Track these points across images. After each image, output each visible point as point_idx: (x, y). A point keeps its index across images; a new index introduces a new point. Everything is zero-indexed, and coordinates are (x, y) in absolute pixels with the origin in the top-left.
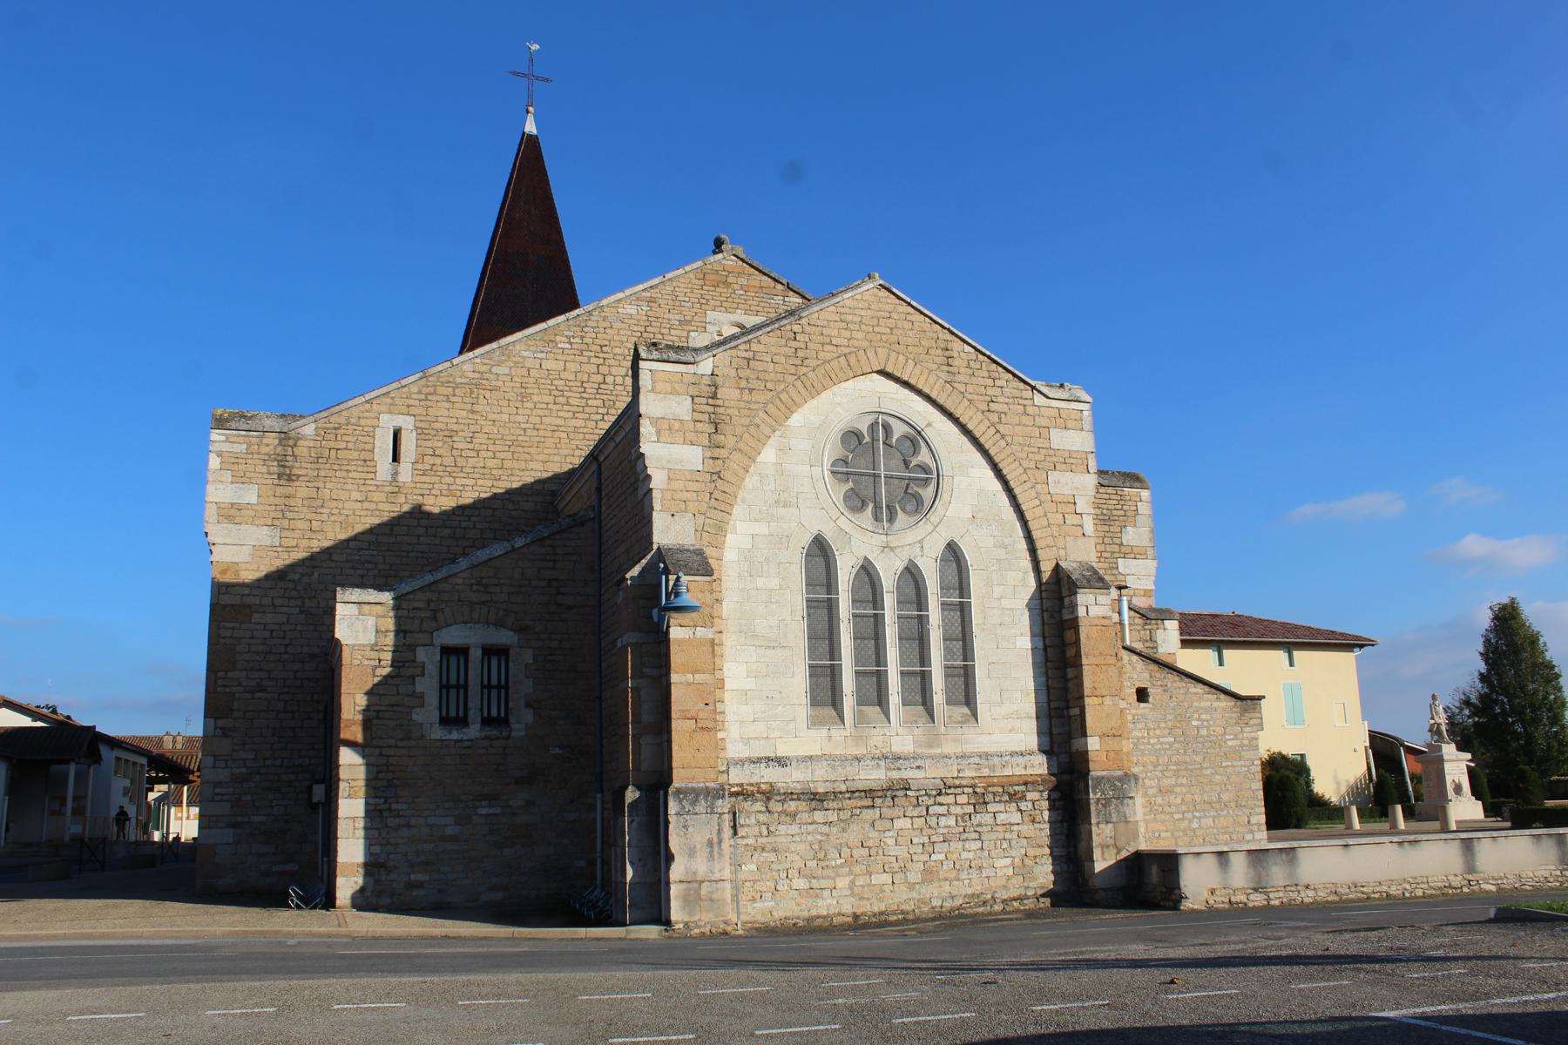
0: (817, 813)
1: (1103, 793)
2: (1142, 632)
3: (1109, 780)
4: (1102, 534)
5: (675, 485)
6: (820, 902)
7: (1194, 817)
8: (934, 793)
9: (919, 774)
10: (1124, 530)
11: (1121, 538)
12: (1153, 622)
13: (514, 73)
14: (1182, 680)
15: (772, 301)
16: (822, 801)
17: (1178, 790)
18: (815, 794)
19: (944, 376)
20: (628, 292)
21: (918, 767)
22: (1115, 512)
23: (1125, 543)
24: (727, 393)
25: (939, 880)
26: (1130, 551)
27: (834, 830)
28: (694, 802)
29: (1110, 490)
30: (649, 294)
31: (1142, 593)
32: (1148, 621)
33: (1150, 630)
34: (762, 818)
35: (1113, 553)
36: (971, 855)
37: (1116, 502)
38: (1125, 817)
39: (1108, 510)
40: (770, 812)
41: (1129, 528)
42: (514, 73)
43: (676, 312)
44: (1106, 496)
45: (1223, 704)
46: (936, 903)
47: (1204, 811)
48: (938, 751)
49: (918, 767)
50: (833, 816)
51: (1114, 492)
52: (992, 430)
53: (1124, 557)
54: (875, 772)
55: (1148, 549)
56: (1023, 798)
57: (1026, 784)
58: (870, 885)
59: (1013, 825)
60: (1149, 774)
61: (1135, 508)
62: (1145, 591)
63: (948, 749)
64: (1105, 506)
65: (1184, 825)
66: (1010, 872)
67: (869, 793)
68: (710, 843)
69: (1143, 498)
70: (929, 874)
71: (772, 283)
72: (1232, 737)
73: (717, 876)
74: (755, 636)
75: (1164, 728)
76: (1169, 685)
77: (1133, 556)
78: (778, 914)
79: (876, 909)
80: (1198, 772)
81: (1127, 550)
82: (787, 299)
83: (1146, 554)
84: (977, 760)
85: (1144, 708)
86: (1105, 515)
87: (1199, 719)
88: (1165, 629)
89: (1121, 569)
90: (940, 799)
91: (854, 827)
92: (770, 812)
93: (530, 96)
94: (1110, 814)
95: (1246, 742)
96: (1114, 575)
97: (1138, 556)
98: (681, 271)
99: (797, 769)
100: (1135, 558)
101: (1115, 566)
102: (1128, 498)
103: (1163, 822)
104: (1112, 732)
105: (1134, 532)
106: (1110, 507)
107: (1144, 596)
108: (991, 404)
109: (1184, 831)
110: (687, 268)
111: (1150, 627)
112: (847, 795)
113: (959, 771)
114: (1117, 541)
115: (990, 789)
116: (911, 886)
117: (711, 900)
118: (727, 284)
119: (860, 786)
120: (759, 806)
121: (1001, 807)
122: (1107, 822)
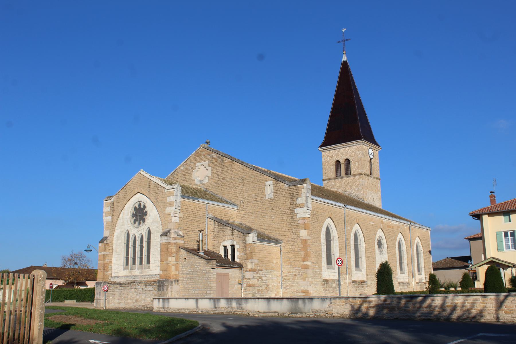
0: (121, 287)
2: (243, 238)
3: (161, 281)
4: (290, 202)
6: (120, 305)
7: (193, 291)
10: (297, 199)
11: (296, 202)
12: (246, 234)
13: (339, 42)
14: (194, 256)
16: (121, 285)
17: (190, 283)
18: (120, 283)
19: (148, 190)
21: (138, 278)
22: (295, 194)
23: (297, 203)
24: (115, 204)
26: (299, 206)
27: (123, 291)
28: (98, 285)
29: (294, 187)
30: (186, 163)
31: (302, 219)
33: (245, 237)
34: (113, 288)
36: (143, 297)
37: (295, 190)
40: (114, 287)
41: (299, 198)
42: (339, 42)
44: (292, 189)
45: (203, 261)
46: (137, 307)
47: (196, 289)
48: (142, 274)
49: (138, 278)
50: (123, 288)
51: (295, 187)
52: (156, 200)
56: (153, 285)
57: (154, 282)
63: (144, 274)
64: (292, 193)
65: (190, 293)
66: (150, 301)
67: (129, 283)
68: (100, 293)
70: (137, 301)
72: (204, 270)
75: (189, 268)
76: (191, 257)
77: (300, 207)
78: (114, 307)
79: (128, 307)
80: (195, 279)
82: (212, 155)
83: (304, 206)
84: (147, 276)
86: (292, 195)
87: (197, 265)
88: (249, 236)
89: (295, 212)
90: (139, 285)
91: (125, 290)
92: (114, 287)
93: (344, 48)
95: (208, 271)
98: (191, 155)
102: (299, 188)
104: (164, 270)
109: (191, 294)
113: (144, 279)
114: (295, 203)
115: (148, 283)
117: (99, 303)
118: (200, 155)
119: (127, 282)
120: (113, 286)
121: (149, 287)
122: (160, 291)
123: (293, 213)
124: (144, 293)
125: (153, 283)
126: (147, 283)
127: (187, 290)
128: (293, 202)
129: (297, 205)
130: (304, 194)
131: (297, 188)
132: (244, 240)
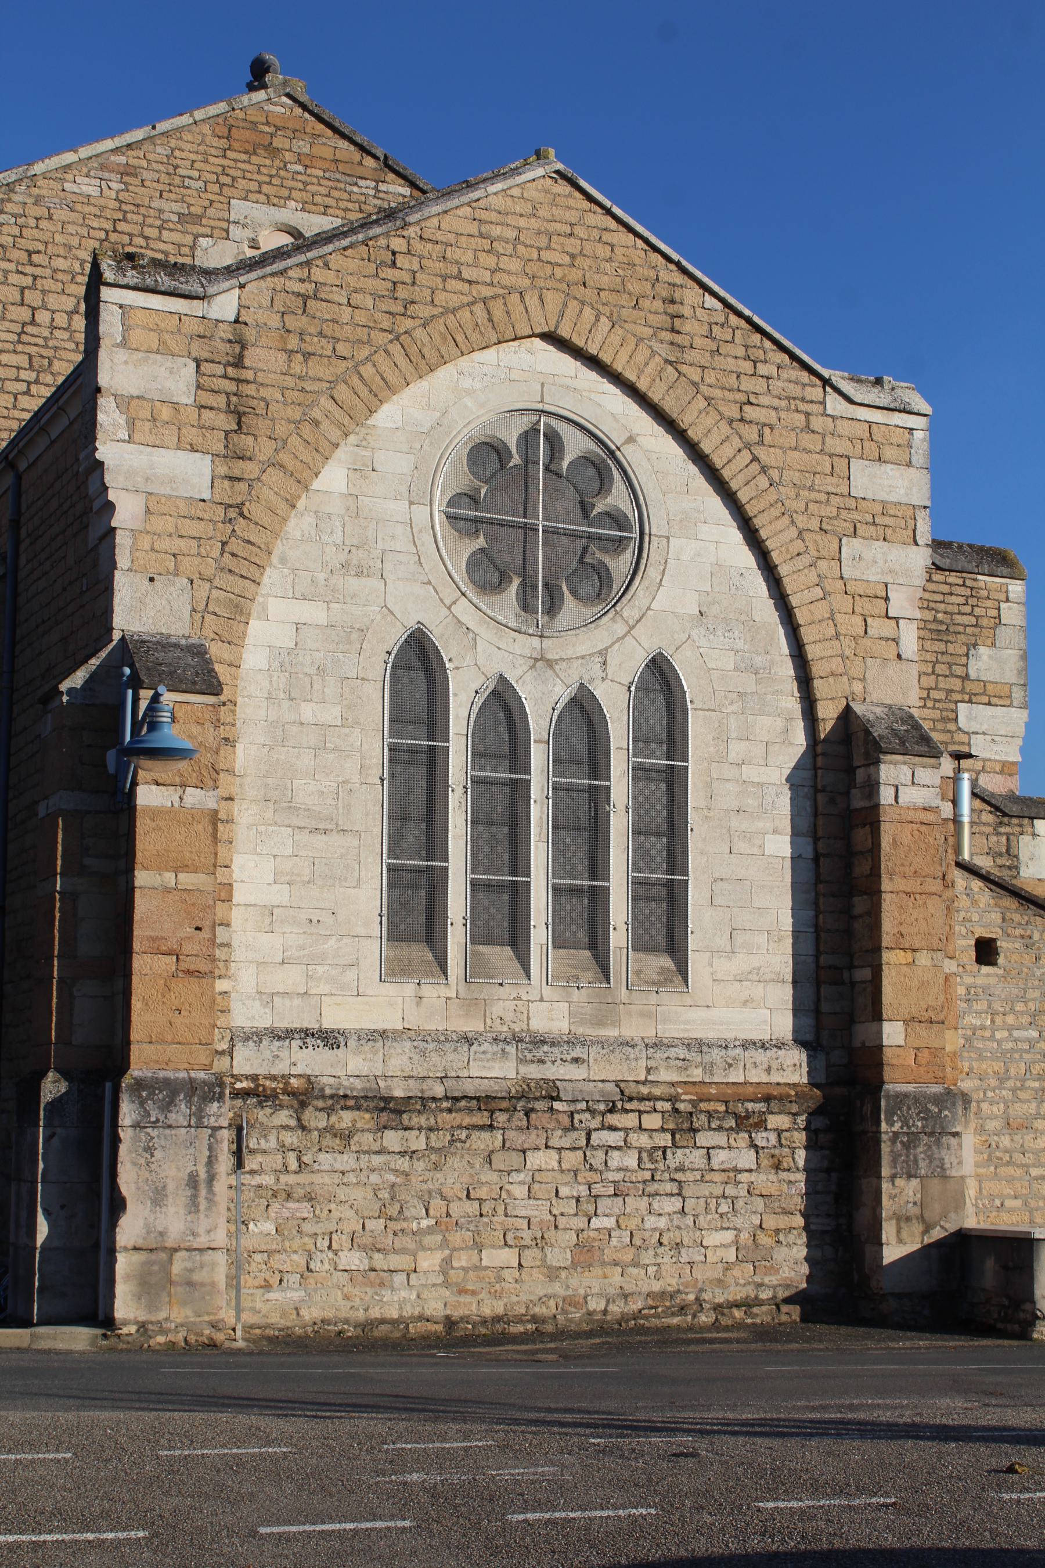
0: (389, 1134)
1: (905, 1123)
2: (993, 839)
3: (916, 1100)
4: (930, 657)
5: (159, 524)
6: (387, 1295)
8: (602, 1107)
9: (577, 1073)
10: (972, 652)
11: (966, 665)
12: (1015, 821)
15: (355, 189)
16: (400, 1112)
19: (664, 350)
20: (84, 152)
21: (576, 1060)
22: (959, 619)
23: (973, 675)
25: (604, 1264)
27: (420, 1165)
28: (167, 1106)
29: (953, 578)
30: (122, 159)
31: (998, 769)
32: (1006, 820)
33: (1008, 835)
34: (291, 1139)
35: (950, 691)
36: (662, 1223)
37: (961, 600)
38: (942, 1167)
39: (945, 613)
40: (303, 1128)
41: (982, 649)
43: (173, 196)
44: (945, 588)
46: (596, 1304)
48: (612, 1033)
49: (576, 1060)
50: (417, 1141)
51: (960, 582)
52: (746, 456)
53: (970, 701)
54: (497, 1065)
55: (1015, 689)
57: (767, 1099)
58: (478, 1268)
59: (740, 1171)
60: (990, 1094)
61: (995, 613)
62: (1004, 764)
63: (632, 1029)
64: (942, 607)
67: (485, 1102)
68: (193, 1181)
69: (1011, 596)
71: (357, 155)
73: (202, 1241)
74: (292, 809)
75: (1022, 1013)
77: (985, 700)
78: (311, 1313)
79: (487, 1312)
81: (976, 688)
82: (382, 187)
83: (1010, 697)
84: (682, 1053)
85: (988, 975)
86: (941, 622)
88: (1034, 835)
89: (962, 722)
90: (613, 1119)
91: (454, 1162)
92: (303, 1128)
94: (916, 1161)
96: (949, 731)
97: (994, 700)
98: (185, 119)
99: (358, 1052)
100: (989, 704)
101: (952, 715)
102: (984, 593)
103: (1010, 1180)
104: (927, 1016)
105: (990, 657)
106: (950, 608)
107: (1002, 772)
108: (747, 408)
110: (199, 115)
111: (1008, 829)
112: (445, 1104)
113: (649, 1070)
114: (959, 671)
115: (703, 1106)
116: (553, 1273)
117: (190, 1284)
118: (273, 152)
119: (470, 1088)
120: (284, 1117)
121: (720, 1139)
122: (910, 1176)
123: (952, 726)
124: (670, 1187)
125: (761, 1106)
126: (694, 1103)
127: (1019, 1172)
128: (950, 665)
129: (969, 686)
130: (1009, 630)
131: (972, 588)
132: (1001, 855)
